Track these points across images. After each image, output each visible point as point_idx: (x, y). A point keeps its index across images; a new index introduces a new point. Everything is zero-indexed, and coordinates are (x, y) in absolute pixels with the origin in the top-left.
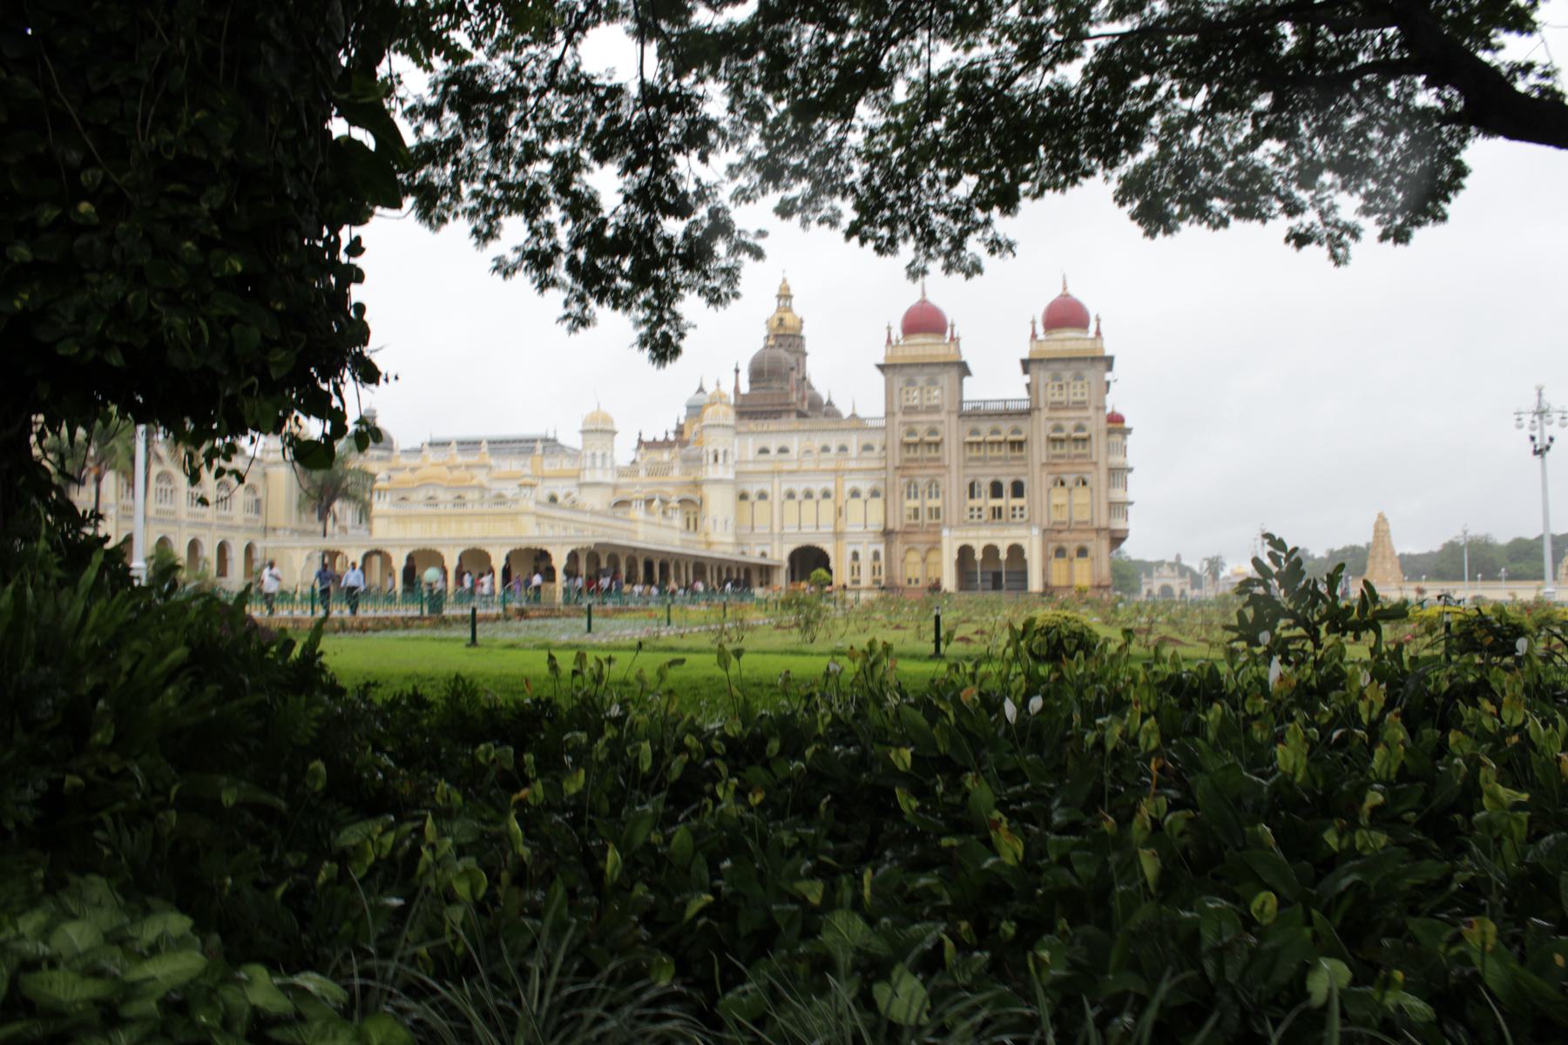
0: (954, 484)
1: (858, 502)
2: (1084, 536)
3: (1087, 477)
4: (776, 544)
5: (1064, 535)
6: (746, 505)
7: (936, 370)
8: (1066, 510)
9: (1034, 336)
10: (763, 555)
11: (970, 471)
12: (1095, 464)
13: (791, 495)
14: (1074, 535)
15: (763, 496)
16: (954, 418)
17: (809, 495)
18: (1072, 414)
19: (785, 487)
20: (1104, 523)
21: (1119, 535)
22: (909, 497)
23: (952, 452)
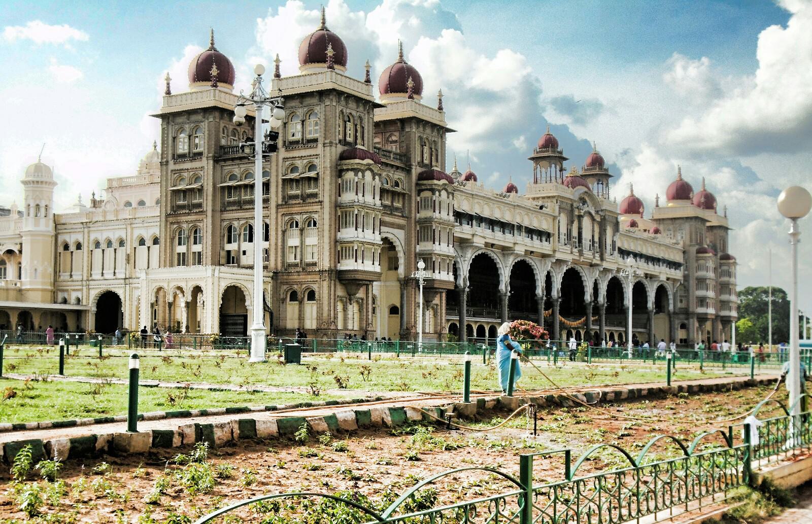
1: (145, 248)
2: (309, 278)
3: (316, 216)
4: (84, 288)
6: (68, 253)
7: (199, 117)
8: (299, 250)
9: (278, 76)
10: (79, 301)
11: (227, 215)
12: (321, 202)
13: (97, 244)
14: (303, 278)
15: (79, 246)
16: (211, 162)
17: (109, 244)
19: (93, 236)
21: (350, 276)
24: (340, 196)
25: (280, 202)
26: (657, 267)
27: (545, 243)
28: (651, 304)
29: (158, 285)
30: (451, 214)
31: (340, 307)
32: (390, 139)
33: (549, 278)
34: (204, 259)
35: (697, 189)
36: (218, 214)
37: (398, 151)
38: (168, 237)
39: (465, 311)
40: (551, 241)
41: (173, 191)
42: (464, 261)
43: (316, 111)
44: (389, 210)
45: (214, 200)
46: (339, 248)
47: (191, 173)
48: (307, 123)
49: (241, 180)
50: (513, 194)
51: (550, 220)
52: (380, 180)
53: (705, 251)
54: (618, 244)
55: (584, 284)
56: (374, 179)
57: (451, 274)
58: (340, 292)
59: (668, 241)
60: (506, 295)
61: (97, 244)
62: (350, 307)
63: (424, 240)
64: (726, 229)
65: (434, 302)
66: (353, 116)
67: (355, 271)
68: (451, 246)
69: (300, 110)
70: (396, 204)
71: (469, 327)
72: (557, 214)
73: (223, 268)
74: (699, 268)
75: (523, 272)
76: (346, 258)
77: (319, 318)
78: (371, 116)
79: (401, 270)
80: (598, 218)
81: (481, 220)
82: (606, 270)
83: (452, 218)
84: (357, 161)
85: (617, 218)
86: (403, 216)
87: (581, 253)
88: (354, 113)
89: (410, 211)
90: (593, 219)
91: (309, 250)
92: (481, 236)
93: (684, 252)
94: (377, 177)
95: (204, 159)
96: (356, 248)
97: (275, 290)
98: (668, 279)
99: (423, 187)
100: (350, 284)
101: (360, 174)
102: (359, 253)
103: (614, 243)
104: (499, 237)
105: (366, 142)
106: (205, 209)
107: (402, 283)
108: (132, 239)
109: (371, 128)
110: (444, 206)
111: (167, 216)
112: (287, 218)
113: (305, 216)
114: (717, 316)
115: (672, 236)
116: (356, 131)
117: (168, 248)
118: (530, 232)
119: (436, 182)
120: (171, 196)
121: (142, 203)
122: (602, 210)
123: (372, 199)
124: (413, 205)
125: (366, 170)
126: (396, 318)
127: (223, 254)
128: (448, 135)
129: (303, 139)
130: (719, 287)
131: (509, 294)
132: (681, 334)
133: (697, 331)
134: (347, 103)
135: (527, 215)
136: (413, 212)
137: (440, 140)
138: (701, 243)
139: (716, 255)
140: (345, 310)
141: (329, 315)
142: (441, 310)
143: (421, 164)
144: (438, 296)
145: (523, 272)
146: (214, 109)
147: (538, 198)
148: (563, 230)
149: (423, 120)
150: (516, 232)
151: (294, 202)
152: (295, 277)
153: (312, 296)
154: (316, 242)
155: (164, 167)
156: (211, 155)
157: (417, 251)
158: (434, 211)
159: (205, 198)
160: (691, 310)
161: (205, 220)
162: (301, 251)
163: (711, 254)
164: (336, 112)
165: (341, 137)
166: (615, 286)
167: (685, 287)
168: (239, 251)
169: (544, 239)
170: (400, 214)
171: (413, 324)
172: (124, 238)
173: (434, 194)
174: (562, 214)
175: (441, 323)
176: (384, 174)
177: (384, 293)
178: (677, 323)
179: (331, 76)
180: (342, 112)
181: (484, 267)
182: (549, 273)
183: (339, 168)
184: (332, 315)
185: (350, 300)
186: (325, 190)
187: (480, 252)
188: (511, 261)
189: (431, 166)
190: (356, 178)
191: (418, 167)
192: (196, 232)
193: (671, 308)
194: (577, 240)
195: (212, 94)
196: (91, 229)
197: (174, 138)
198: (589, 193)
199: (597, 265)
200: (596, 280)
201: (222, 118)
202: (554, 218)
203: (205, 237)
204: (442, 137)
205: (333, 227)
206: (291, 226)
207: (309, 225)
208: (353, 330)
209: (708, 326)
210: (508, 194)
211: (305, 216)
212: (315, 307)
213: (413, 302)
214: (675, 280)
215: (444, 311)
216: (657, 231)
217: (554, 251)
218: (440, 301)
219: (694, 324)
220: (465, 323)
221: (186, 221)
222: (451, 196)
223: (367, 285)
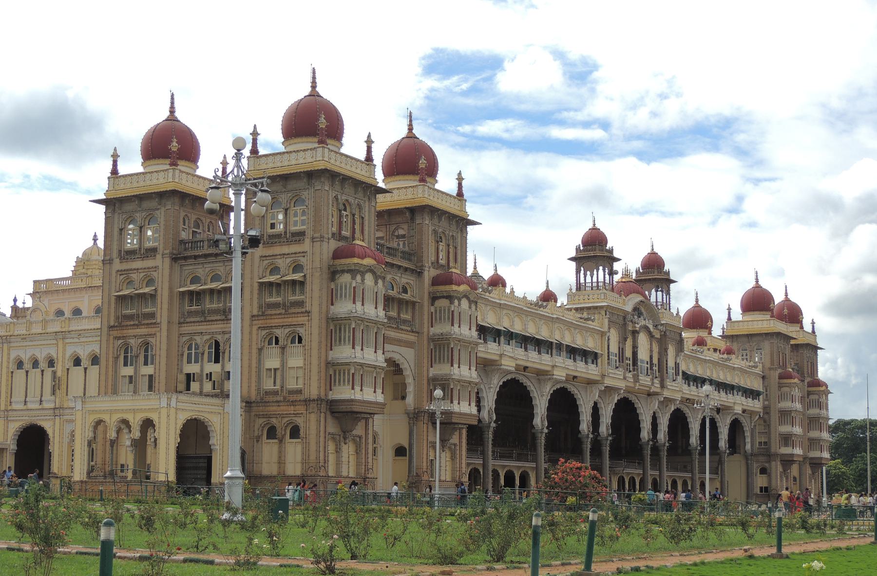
0: (164, 347)
1: (80, 369)
3: (301, 331)
5: (273, 409)
7: (154, 204)
8: (278, 374)
9: (254, 151)
11: (187, 329)
13: (20, 365)
14: (284, 409)
16: (167, 261)
17: (35, 364)
18: (286, 250)
19: (13, 355)
20: (314, 391)
21: (343, 408)
22: (125, 364)
23: (163, 310)
24: (332, 304)
25: (255, 312)
26: (730, 396)
27: (593, 366)
28: (723, 443)
29: (97, 417)
30: (474, 328)
31: (331, 447)
32: (396, 234)
33: (596, 410)
34: (157, 385)
35: (778, 298)
36: (175, 327)
37: (407, 249)
38: (111, 356)
39: (490, 453)
40: (599, 364)
41: (118, 297)
42: (490, 388)
43: (303, 197)
44: (395, 323)
45: (170, 310)
46: (331, 372)
47: (142, 274)
48: (291, 213)
49: (205, 284)
50: (551, 303)
51: (597, 337)
52: (383, 285)
53: (790, 377)
54: (683, 367)
55: (640, 418)
56: (376, 283)
57: (473, 404)
58: (332, 428)
59: (743, 364)
60: (542, 433)
61: (20, 365)
62: (345, 448)
63: (440, 362)
64: (815, 348)
65: (452, 441)
66: (350, 205)
67: (352, 400)
68: (473, 368)
69: (283, 196)
70: (404, 316)
71: (496, 474)
72: (606, 329)
73: (182, 397)
74: (782, 397)
75: (563, 402)
76: (340, 384)
77: (304, 462)
78: (373, 204)
79: (410, 399)
80: (658, 336)
81: (510, 336)
82: (668, 401)
83: (475, 334)
84: (356, 260)
85: (681, 335)
86: (413, 332)
87: (636, 379)
88: (351, 200)
89: (422, 324)
90: (651, 336)
91: (293, 373)
92: (511, 358)
93: (763, 377)
94: (380, 281)
95: (159, 257)
96: (352, 371)
97: (248, 426)
98: (744, 411)
99: (438, 295)
100: (346, 418)
101: (359, 278)
102: (357, 378)
103: (677, 365)
104: (534, 358)
105: (366, 237)
106: (159, 321)
107: (411, 416)
108: (64, 358)
109: (373, 218)
110: (465, 318)
111: (111, 327)
112: (264, 332)
113: (287, 330)
114: (805, 458)
115: (748, 357)
116: (354, 223)
117: (110, 369)
118: (573, 352)
119: (454, 287)
120: (116, 303)
121: (77, 312)
122: (662, 325)
123: (374, 311)
124: (426, 317)
125: (367, 272)
126: (404, 461)
127: (182, 378)
128: (470, 228)
129: (286, 232)
130: (807, 421)
131: (546, 431)
132: (761, 481)
133: (781, 477)
134: (342, 187)
135: (570, 331)
136: (426, 325)
137: (459, 235)
138: (784, 366)
139: (803, 381)
140: (338, 451)
141: (318, 458)
142: (461, 450)
143: (436, 264)
144: (457, 433)
145: (563, 402)
146: (174, 193)
147: (582, 309)
148: (614, 349)
149: (437, 210)
150: (554, 351)
151: (273, 312)
152: (273, 409)
153: (295, 433)
154: (300, 363)
155: (108, 266)
156: (167, 251)
157: (431, 375)
158: (453, 325)
159: (159, 306)
160: (773, 450)
161: (158, 334)
162: (282, 376)
163: (796, 380)
164: (328, 199)
165: (334, 229)
166: (679, 421)
167: (765, 421)
168: (201, 375)
169: (590, 361)
170: (409, 329)
171: (425, 470)
172: (55, 356)
173: (452, 303)
174: (612, 330)
175: (461, 467)
176: (389, 277)
177: (388, 430)
178: (756, 467)
179: (323, 153)
180: (336, 198)
181: (514, 395)
182: (595, 403)
183: (332, 269)
184: (322, 458)
185: (345, 438)
186: (314, 294)
187: (509, 377)
188: (548, 389)
189: (449, 268)
190: (354, 282)
191: (432, 269)
192: (146, 351)
193: (748, 447)
194: (631, 362)
195: (170, 175)
196: (12, 345)
197: (121, 230)
198: (645, 302)
199: (656, 394)
200: (654, 413)
201: (182, 205)
202: (603, 334)
203: (158, 357)
204: (464, 232)
205: (324, 343)
206: (270, 343)
207: (293, 342)
208: (348, 477)
209: (794, 470)
210: (545, 304)
211: (287, 330)
212: (299, 448)
213: (425, 442)
214: (752, 413)
215: (464, 453)
216: (729, 352)
217: (603, 376)
218: (459, 439)
219: (777, 468)
220: (491, 469)
221: (135, 335)
222: (473, 307)
223: (367, 419)
